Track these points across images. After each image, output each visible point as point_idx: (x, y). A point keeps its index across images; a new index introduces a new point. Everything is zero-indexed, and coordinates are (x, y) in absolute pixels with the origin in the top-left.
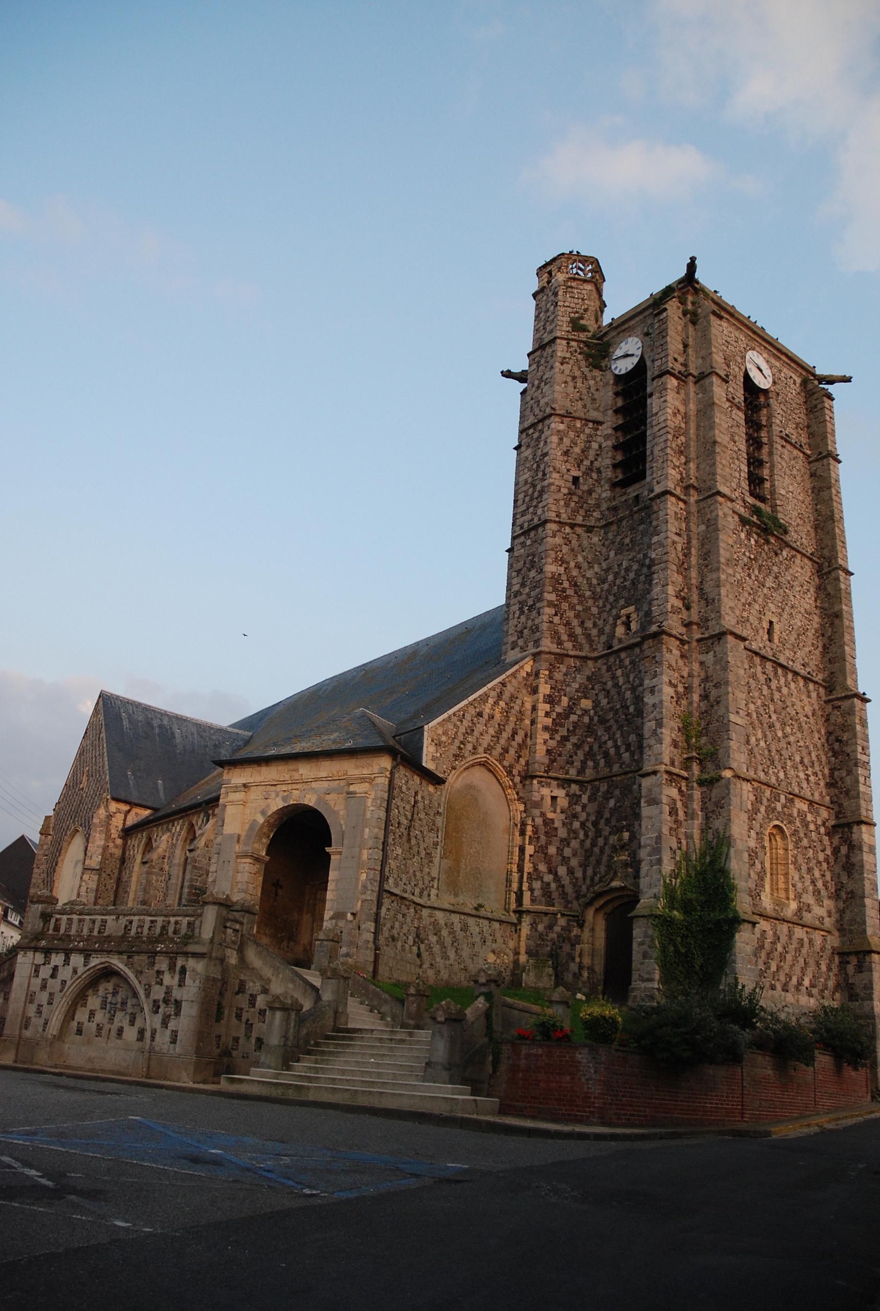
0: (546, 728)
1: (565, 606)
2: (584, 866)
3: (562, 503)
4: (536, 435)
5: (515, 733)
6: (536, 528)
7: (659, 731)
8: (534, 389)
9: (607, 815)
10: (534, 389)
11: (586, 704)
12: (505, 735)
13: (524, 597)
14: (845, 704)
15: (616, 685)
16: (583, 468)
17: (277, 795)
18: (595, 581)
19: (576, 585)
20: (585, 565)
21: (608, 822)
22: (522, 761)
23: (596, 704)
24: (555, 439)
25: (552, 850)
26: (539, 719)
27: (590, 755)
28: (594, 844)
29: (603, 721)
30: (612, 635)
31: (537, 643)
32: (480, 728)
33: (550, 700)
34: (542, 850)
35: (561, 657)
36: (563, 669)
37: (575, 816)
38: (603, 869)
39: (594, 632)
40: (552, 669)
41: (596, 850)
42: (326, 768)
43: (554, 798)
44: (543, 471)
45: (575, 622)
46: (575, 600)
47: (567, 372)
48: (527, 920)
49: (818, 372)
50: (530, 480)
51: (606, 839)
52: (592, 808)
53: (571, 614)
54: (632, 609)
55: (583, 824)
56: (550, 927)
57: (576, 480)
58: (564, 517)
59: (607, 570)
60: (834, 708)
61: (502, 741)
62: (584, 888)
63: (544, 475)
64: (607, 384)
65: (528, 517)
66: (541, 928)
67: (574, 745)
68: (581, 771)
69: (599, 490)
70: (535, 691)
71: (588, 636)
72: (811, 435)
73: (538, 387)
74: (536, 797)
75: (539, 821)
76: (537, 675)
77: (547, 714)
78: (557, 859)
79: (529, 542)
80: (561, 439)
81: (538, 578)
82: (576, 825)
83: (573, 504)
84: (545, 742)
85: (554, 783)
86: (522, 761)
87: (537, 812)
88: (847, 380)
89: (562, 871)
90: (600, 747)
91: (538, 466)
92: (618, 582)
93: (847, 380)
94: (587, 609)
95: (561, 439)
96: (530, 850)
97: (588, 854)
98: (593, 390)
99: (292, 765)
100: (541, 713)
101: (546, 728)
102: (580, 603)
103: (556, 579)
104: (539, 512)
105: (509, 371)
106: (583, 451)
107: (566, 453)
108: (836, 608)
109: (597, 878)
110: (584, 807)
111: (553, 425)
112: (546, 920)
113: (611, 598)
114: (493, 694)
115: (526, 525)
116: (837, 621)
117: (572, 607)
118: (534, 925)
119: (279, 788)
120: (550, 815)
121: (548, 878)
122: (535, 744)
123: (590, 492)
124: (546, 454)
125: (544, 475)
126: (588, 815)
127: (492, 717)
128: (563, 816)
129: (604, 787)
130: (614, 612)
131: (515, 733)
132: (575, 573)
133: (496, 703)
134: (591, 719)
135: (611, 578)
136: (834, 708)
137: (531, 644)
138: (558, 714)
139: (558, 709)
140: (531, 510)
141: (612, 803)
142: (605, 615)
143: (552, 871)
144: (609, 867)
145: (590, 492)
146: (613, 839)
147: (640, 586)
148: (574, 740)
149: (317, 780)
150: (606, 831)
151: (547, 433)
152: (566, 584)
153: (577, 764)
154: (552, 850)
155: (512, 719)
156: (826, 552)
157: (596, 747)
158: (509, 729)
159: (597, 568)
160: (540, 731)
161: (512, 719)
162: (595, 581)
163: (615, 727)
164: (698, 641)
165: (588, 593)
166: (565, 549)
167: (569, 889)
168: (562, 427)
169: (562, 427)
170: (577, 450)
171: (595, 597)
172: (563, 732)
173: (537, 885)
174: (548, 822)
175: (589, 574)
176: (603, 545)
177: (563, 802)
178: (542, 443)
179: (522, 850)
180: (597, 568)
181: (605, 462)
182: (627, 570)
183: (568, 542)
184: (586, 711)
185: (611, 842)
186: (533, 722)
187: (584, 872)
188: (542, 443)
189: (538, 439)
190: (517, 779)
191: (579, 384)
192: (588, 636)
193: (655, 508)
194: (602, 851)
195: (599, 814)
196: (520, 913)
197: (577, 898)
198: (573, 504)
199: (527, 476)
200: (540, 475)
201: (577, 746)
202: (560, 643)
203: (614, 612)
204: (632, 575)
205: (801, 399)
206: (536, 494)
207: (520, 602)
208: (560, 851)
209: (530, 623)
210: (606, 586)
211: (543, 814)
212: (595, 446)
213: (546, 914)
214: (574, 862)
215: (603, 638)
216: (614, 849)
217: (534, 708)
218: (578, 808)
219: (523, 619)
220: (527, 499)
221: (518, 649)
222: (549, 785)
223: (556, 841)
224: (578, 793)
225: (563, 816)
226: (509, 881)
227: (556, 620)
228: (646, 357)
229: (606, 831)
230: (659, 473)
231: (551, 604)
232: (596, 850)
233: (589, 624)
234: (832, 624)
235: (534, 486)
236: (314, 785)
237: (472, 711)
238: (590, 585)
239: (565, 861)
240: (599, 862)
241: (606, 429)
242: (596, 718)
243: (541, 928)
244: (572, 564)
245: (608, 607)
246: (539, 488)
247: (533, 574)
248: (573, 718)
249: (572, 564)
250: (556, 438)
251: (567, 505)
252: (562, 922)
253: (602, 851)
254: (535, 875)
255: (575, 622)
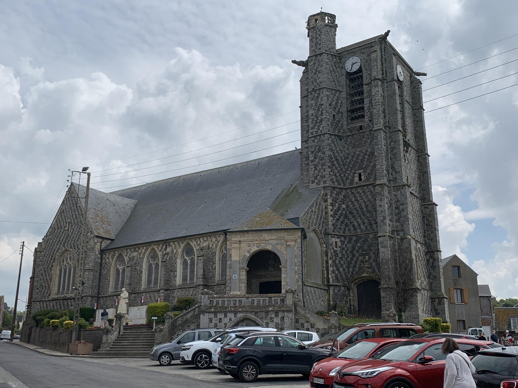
0: (331, 216)
1: (334, 168)
2: (348, 268)
3: (330, 126)
4: (316, 95)
5: (321, 218)
6: (320, 135)
7: (384, 221)
8: (313, 74)
9: (357, 248)
10: (313, 74)
11: (344, 206)
12: (319, 218)
13: (316, 163)
14: (429, 207)
15: (357, 200)
16: (336, 111)
17: (254, 245)
18: (343, 158)
19: (337, 160)
20: (340, 152)
21: (357, 251)
22: (324, 228)
23: (347, 206)
24: (326, 98)
25: (337, 262)
26: (329, 212)
27: (347, 225)
28: (352, 259)
29: (351, 213)
30: (353, 180)
31: (325, 182)
32: (313, 216)
33: (332, 205)
34: (334, 262)
35: (334, 188)
36: (335, 192)
37: (343, 249)
38: (357, 269)
39: (344, 178)
40: (332, 193)
41: (353, 262)
42: (274, 236)
43: (336, 242)
44: (322, 112)
45: (338, 174)
46: (337, 165)
47: (328, 69)
48: (332, 288)
49: (414, 71)
50: (314, 114)
51: (357, 258)
52: (350, 246)
53: (336, 171)
54: (362, 171)
55: (346, 252)
56: (339, 291)
57: (334, 115)
58: (331, 132)
59: (348, 154)
60: (425, 208)
61: (318, 221)
62: (349, 276)
63: (322, 113)
64: (343, 75)
65: (315, 130)
66: (336, 291)
67: (341, 222)
68: (344, 232)
69: (342, 120)
70: (326, 201)
71: (342, 180)
72: (413, 98)
73: (315, 73)
74: (330, 242)
75: (332, 251)
76: (326, 195)
77: (331, 210)
78: (339, 265)
79: (316, 141)
80: (328, 98)
81: (323, 156)
82: (344, 252)
83: (333, 126)
84: (332, 221)
85: (336, 237)
86: (324, 228)
87: (331, 247)
88: (425, 75)
89: (341, 270)
90: (351, 223)
91: (319, 109)
92: (354, 159)
93: (425, 75)
94: (341, 169)
95: (328, 98)
96: (330, 262)
97: (350, 263)
98: (338, 76)
99: (259, 233)
100: (329, 210)
101: (331, 216)
102: (339, 167)
103: (330, 157)
104: (321, 129)
105: (295, 61)
106: (336, 104)
107: (330, 105)
108: (425, 170)
109: (355, 272)
110: (346, 245)
111: (324, 92)
112: (338, 289)
113: (351, 166)
114: (315, 203)
115: (314, 133)
116: (425, 175)
117: (336, 168)
118: (334, 290)
119: (254, 242)
120: (335, 249)
121: (337, 272)
122: (328, 222)
123: (339, 121)
124: (322, 105)
125: (322, 113)
126: (348, 248)
127: (315, 212)
128: (340, 249)
129: (354, 238)
130: (353, 171)
131: (321, 218)
132: (336, 154)
133: (316, 207)
134: (346, 212)
135: (350, 157)
136: (425, 208)
137: (322, 183)
138: (335, 210)
139: (335, 208)
140: (316, 127)
141: (359, 244)
142: (349, 172)
143: (338, 270)
144: (360, 268)
145: (339, 121)
146: (361, 258)
147: (365, 163)
148: (341, 220)
149: (271, 240)
150: (357, 255)
151: (321, 95)
152: (334, 159)
153: (343, 229)
154: (337, 262)
155: (320, 212)
156: (420, 147)
157: (349, 223)
158: (320, 216)
159: (344, 153)
160: (330, 217)
161: (320, 212)
162: (343, 158)
163: (357, 216)
164: (393, 187)
165: (341, 163)
166: (333, 145)
167: (344, 276)
168: (328, 93)
169: (328, 93)
170: (334, 103)
171: (344, 165)
172: (337, 217)
173: (334, 275)
174: (335, 251)
175: (341, 155)
176: (346, 143)
177: (339, 244)
178: (320, 100)
179: (327, 262)
180: (344, 153)
181: (344, 109)
182: (358, 155)
183: (333, 142)
184: (344, 209)
185: (360, 259)
186: (326, 213)
187: (348, 270)
188: (320, 100)
189: (318, 97)
190: (323, 235)
191: (333, 75)
192: (342, 180)
193: (376, 135)
194: (356, 262)
195: (353, 248)
196: (329, 286)
197: (347, 280)
198: (333, 126)
199: (313, 112)
200: (320, 113)
201: (342, 222)
202: (333, 183)
203: (353, 171)
204: (361, 158)
205: (409, 83)
206: (318, 121)
207: (314, 165)
208: (340, 262)
209: (320, 174)
210: (348, 160)
211: (333, 248)
212: (340, 101)
213: (337, 286)
214: (345, 267)
215: (348, 181)
216: (362, 261)
217: (326, 208)
218: (344, 246)
219: (316, 172)
220: (314, 122)
221: (315, 184)
222: (334, 237)
223: (338, 258)
224: (343, 240)
225: (340, 249)
226: (323, 273)
227: (331, 173)
228: (363, 67)
229: (357, 255)
230: (377, 120)
231: (329, 167)
232: (353, 262)
233: (342, 175)
234: (423, 176)
235: (317, 117)
236: (270, 241)
237: (310, 210)
238: (342, 159)
239: (342, 266)
240: (355, 266)
241: (344, 95)
242: (348, 212)
243: (336, 291)
244: (335, 151)
245: (350, 169)
246: (319, 118)
247: (320, 154)
248: (340, 212)
249: (335, 151)
250: (325, 98)
251: (332, 127)
252: (343, 288)
253: (356, 262)
254: (333, 272)
255: (338, 174)
